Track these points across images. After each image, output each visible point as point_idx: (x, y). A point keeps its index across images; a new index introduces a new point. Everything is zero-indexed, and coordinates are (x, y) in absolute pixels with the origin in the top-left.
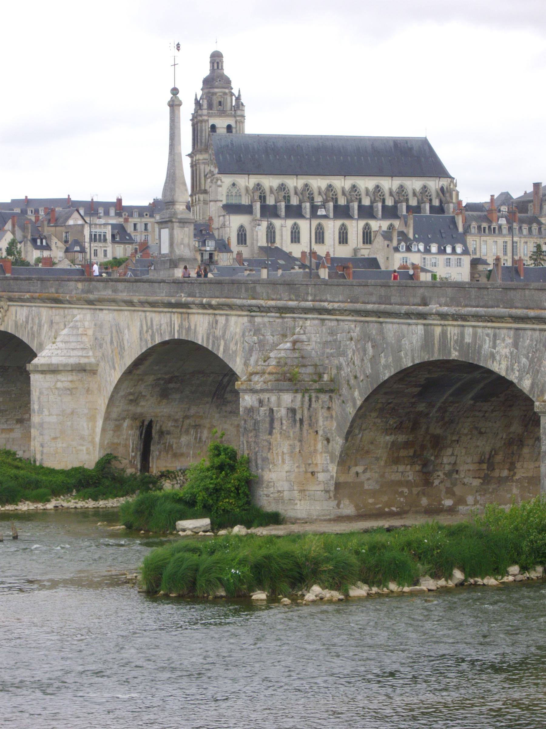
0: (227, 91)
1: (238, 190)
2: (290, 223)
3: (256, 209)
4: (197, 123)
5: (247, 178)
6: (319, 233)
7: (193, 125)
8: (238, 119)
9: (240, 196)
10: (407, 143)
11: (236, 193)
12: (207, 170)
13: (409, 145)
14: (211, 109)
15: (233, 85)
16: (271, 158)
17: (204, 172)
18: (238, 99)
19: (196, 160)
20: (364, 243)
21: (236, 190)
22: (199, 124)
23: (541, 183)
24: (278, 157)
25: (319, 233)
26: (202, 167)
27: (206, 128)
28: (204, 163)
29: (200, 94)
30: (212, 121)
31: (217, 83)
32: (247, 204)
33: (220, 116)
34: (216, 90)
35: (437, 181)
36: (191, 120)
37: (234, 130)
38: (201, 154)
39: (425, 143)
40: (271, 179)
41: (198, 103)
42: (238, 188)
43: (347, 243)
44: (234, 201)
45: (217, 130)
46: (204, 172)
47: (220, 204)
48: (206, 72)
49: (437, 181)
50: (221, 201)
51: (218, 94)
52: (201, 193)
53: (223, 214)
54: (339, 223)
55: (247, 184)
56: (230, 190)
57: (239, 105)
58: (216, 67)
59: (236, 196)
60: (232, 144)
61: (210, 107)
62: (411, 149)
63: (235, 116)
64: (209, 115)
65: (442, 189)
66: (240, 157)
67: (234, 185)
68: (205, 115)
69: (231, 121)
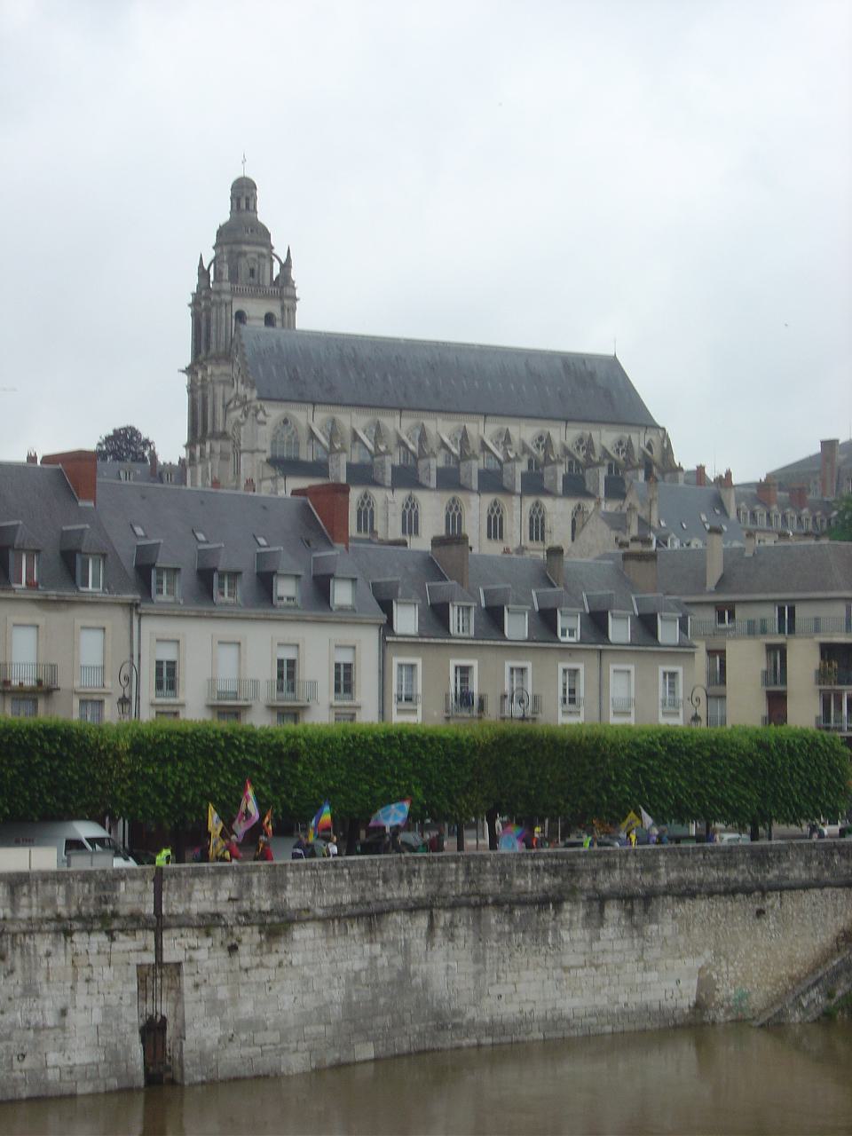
0: (264, 251)
1: (293, 433)
2: (401, 496)
3: (338, 465)
4: (208, 310)
5: (310, 411)
6: (454, 516)
7: (196, 317)
8: (286, 302)
9: (297, 443)
10: (584, 363)
11: (289, 437)
12: (231, 394)
13: (589, 367)
14: (237, 283)
15: (273, 242)
16: (352, 376)
17: (224, 398)
18: (286, 266)
19: (203, 379)
20: (531, 538)
21: (289, 434)
22: (214, 310)
23: (838, 441)
24: (364, 376)
25: (454, 516)
26: (219, 389)
27: (227, 315)
28: (224, 383)
29: (209, 255)
30: (237, 306)
31: (247, 235)
32: (310, 459)
33: (253, 296)
34: (246, 248)
35: (642, 434)
36: (190, 305)
37: (278, 324)
38: (218, 364)
39: (613, 363)
40: (354, 414)
41: (203, 273)
42: (293, 428)
43: (501, 537)
44: (285, 453)
45: (248, 322)
46: (224, 398)
47: (264, 457)
48: (223, 214)
49: (642, 434)
50: (265, 452)
51: (249, 256)
52: (217, 439)
53: (273, 474)
54: (488, 499)
55: (310, 421)
56: (279, 431)
57: (285, 281)
58: (243, 205)
59: (288, 443)
60: (279, 346)
61: (234, 277)
62: (592, 375)
63: (281, 298)
64: (233, 293)
65: (649, 447)
66: (295, 370)
67: (286, 422)
68: (225, 292)
69: (275, 308)
